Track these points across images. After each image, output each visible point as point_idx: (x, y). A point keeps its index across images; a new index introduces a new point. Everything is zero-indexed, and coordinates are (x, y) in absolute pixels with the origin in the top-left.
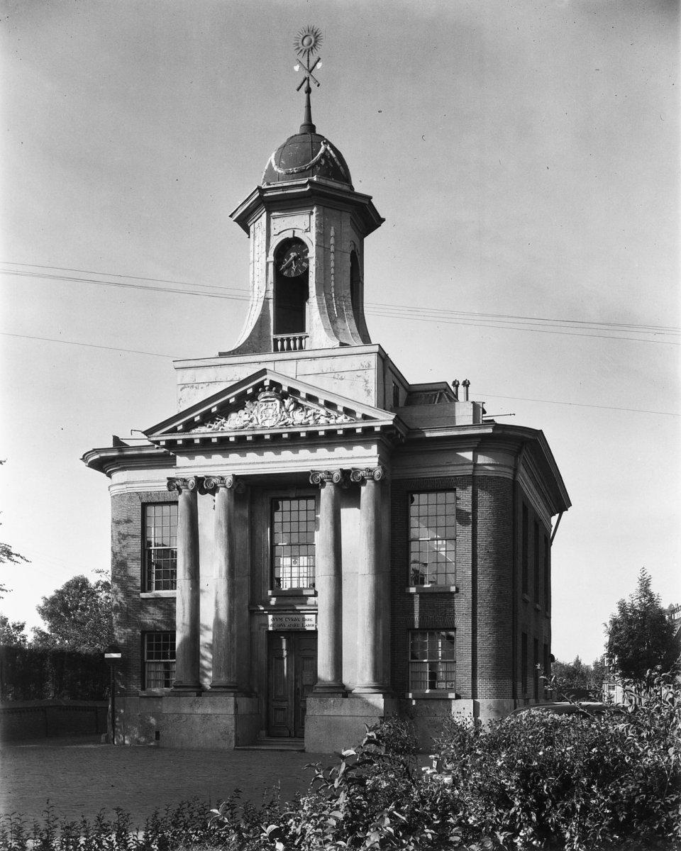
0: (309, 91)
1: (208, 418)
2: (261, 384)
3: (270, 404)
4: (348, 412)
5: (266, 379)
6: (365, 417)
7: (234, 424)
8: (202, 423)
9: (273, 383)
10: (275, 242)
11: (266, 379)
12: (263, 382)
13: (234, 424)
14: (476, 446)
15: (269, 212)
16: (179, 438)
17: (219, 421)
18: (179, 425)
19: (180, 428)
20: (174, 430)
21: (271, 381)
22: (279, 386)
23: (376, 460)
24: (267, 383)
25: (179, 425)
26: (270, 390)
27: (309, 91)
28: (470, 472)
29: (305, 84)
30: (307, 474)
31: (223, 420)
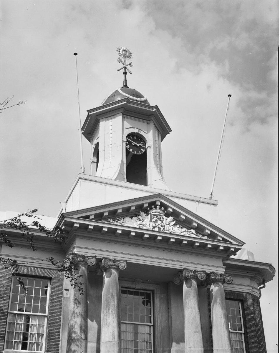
0: (125, 73)
1: (114, 215)
2: (154, 203)
3: (159, 217)
5: (158, 201)
8: (106, 219)
9: (162, 205)
10: (127, 132)
11: (158, 201)
12: (155, 202)
14: (253, 276)
15: (123, 114)
16: (92, 225)
17: (118, 220)
18: (106, 212)
20: (87, 217)
21: (161, 203)
22: (166, 207)
23: (224, 270)
24: (158, 203)
25: (106, 212)
27: (125, 73)
29: (123, 70)
31: (122, 221)
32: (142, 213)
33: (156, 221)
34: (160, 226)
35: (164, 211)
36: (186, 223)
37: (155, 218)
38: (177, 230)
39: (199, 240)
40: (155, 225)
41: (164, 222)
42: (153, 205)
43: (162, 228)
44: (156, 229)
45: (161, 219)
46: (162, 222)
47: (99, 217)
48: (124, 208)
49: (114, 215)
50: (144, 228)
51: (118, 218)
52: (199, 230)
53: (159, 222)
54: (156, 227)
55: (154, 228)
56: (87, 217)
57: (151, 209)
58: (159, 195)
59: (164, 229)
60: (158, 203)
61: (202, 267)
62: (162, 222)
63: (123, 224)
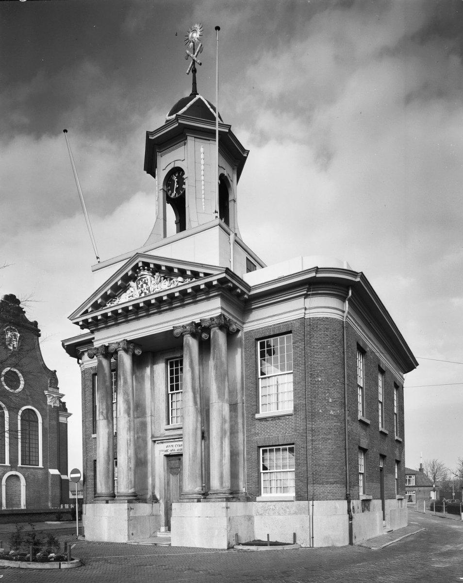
1: (107, 298)
2: (136, 266)
4: (195, 275)
6: (206, 275)
7: (125, 299)
9: (146, 264)
12: (137, 264)
13: (125, 299)
19: (90, 310)
20: (86, 312)
24: (140, 264)
26: (144, 269)
28: (303, 316)
30: (172, 331)
31: (118, 300)
32: (132, 283)
33: (142, 286)
34: (146, 291)
35: (148, 270)
36: (169, 274)
37: (141, 283)
38: (165, 285)
39: (176, 285)
40: (141, 290)
41: (149, 284)
42: (136, 268)
43: (147, 292)
44: (143, 295)
45: (146, 281)
46: (147, 284)
47: (96, 306)
48: (111, 287)
49: (107, 298)
50: (133, 299)
51: (114, 300)
52: (182, 273)
53: (144, 285)
54: (142, 293)
55: (140, 295)
56: (86, 312)
57: (137, 273)
58: (138, 255)
59: (149, 291)
60: (140, 264)
61: (187, 319)
62: (147, 284)
63: (120, 303)
